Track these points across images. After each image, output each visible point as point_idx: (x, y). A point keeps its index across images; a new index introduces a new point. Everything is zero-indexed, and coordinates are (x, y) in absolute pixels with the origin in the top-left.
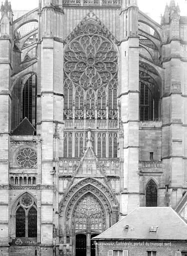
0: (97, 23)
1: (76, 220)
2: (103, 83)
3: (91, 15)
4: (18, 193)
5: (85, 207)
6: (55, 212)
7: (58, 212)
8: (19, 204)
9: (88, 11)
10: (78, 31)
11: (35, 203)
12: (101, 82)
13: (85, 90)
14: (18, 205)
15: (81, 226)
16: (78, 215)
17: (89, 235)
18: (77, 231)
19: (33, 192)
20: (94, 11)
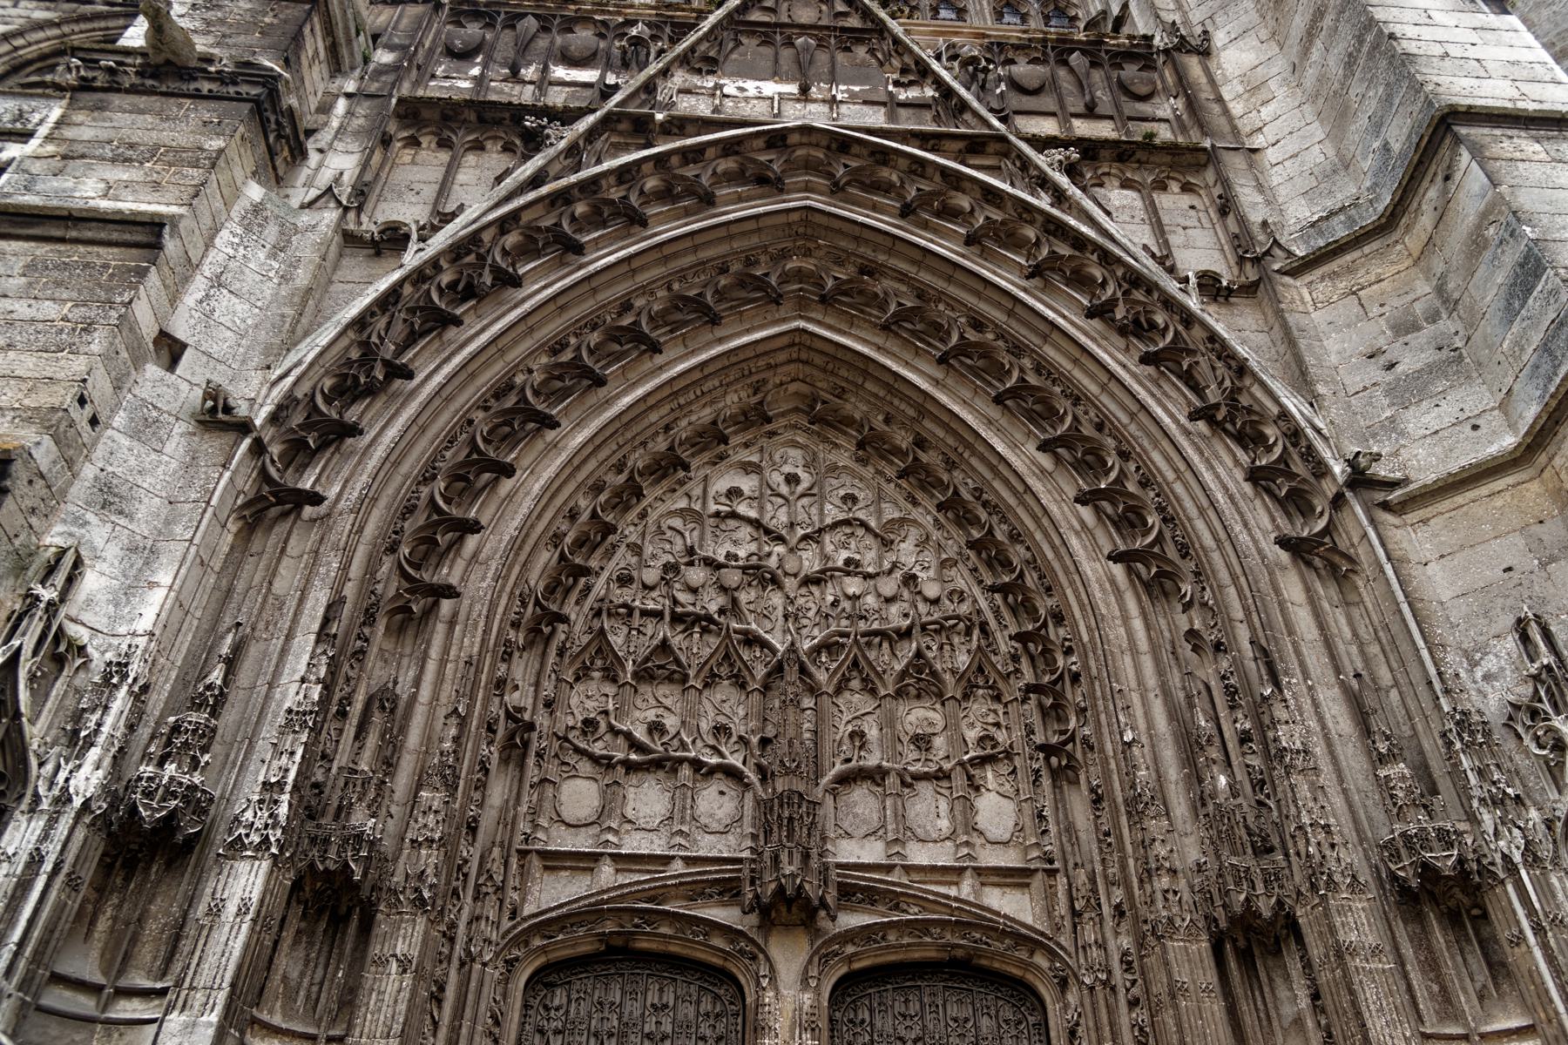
1: (587, 699)
16: (617, 641)
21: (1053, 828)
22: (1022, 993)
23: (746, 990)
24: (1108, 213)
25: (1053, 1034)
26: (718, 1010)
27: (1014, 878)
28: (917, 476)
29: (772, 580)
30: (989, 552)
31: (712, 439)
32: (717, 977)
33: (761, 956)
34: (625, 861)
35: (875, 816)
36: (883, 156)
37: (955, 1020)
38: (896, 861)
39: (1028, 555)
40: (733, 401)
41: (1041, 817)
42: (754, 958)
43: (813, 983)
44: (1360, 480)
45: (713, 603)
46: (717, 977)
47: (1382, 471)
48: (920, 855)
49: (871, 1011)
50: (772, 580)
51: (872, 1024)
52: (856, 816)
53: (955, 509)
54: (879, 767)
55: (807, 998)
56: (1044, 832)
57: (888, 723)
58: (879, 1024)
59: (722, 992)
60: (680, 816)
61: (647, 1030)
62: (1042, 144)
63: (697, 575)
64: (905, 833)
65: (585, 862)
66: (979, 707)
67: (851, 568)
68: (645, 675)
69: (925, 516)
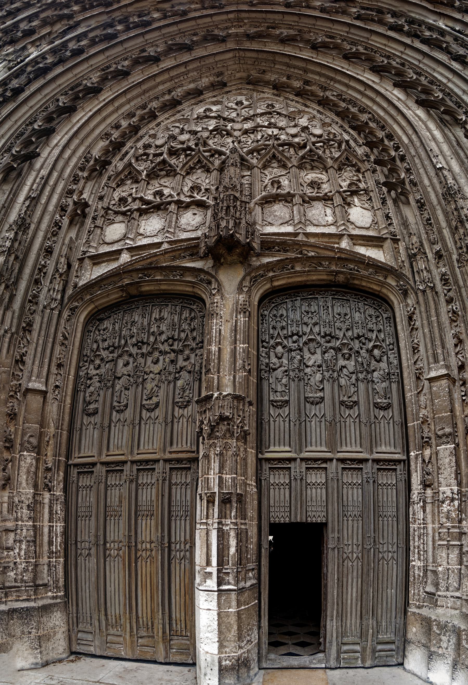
21: (395, 221)
23: (206, 302)
25: (398, 320)
26: (193, 315)
33: (213, 280)
35: (287, 216)
37: (339, 315)
38: (300, 231)
39: (370, 115)
41: (388, 217)
42: (210, 283)
43: (245, 289)
49: (287, 310)
51: (287, 316)
52: (275, 216)
54: (289, 193)
55: (242, 298)
56: (390, 225)
58: (291, 315)
59: (195, 307)
61: (152, 330)
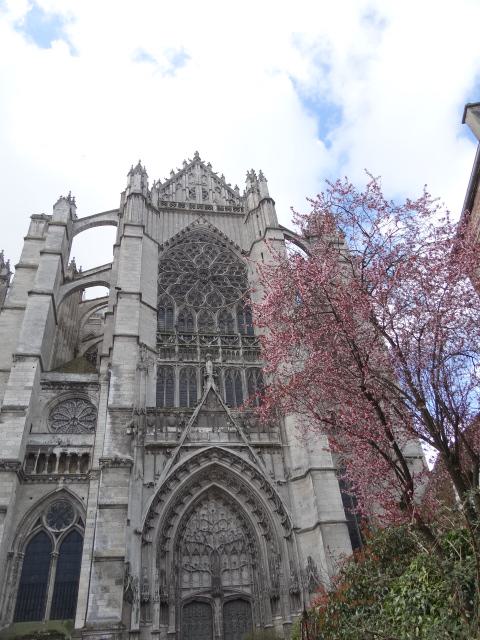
0: (211, 231)
1: (185, 560)
2: (227, 302)
3: (201, 223)
4: (39, 491)
5: (205, 527)
6: (131, 530)
7: (141, 530)
8: (39, 521)
9: (196, 217)
10: (180, 240)
11: (80, 522)
12: (224, 301)
13: (197, 311)
14: (36, 526)
15: (196, 577)
17: (218, 601)
18: (185, 595)
19: (74, 488)
20: (206, 217)
22: (248, 602)
24: (264, 463)
27: (247, 586)
28: (234, 511)
29: (210, 533)
30: (245, 526)
31: (200, 505)
32: (208, 604)
34: (194, 589)
36: (227, 452)
40: (202, 497)
44: (295, 529)
45: (202, 539)
46: (208, 604)
47: (299, 526)
48: (235, 583)
50: (210, 533)
53: (240, 518)
57: (229, 560)
60: (201, 579)
62: (256, 446)
63: (200, 533)
64: (233, 579)
65: (189, 589)
66: (243, 556)
67: (223, 530)
68: (194, 555)
69: (234, 517)
